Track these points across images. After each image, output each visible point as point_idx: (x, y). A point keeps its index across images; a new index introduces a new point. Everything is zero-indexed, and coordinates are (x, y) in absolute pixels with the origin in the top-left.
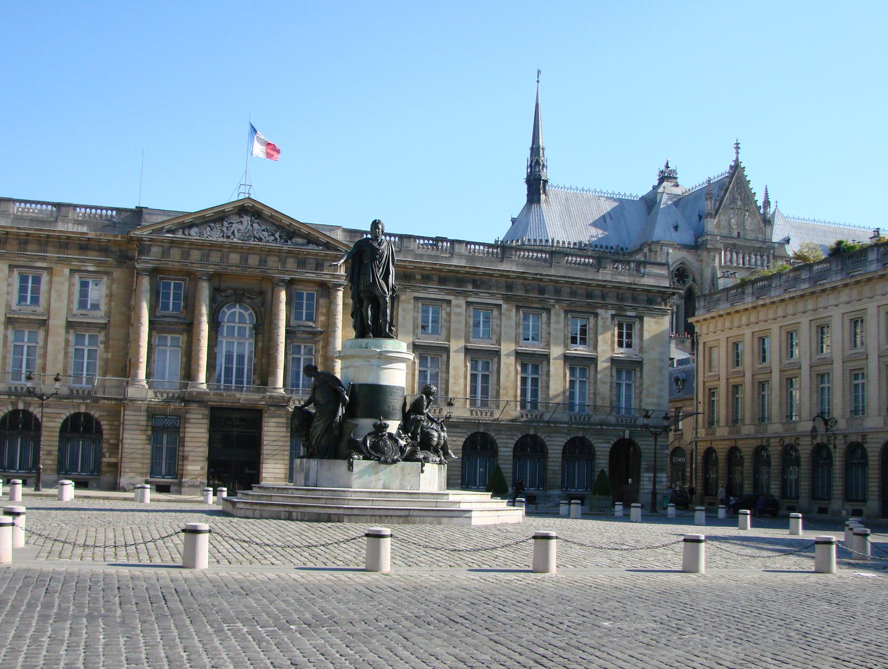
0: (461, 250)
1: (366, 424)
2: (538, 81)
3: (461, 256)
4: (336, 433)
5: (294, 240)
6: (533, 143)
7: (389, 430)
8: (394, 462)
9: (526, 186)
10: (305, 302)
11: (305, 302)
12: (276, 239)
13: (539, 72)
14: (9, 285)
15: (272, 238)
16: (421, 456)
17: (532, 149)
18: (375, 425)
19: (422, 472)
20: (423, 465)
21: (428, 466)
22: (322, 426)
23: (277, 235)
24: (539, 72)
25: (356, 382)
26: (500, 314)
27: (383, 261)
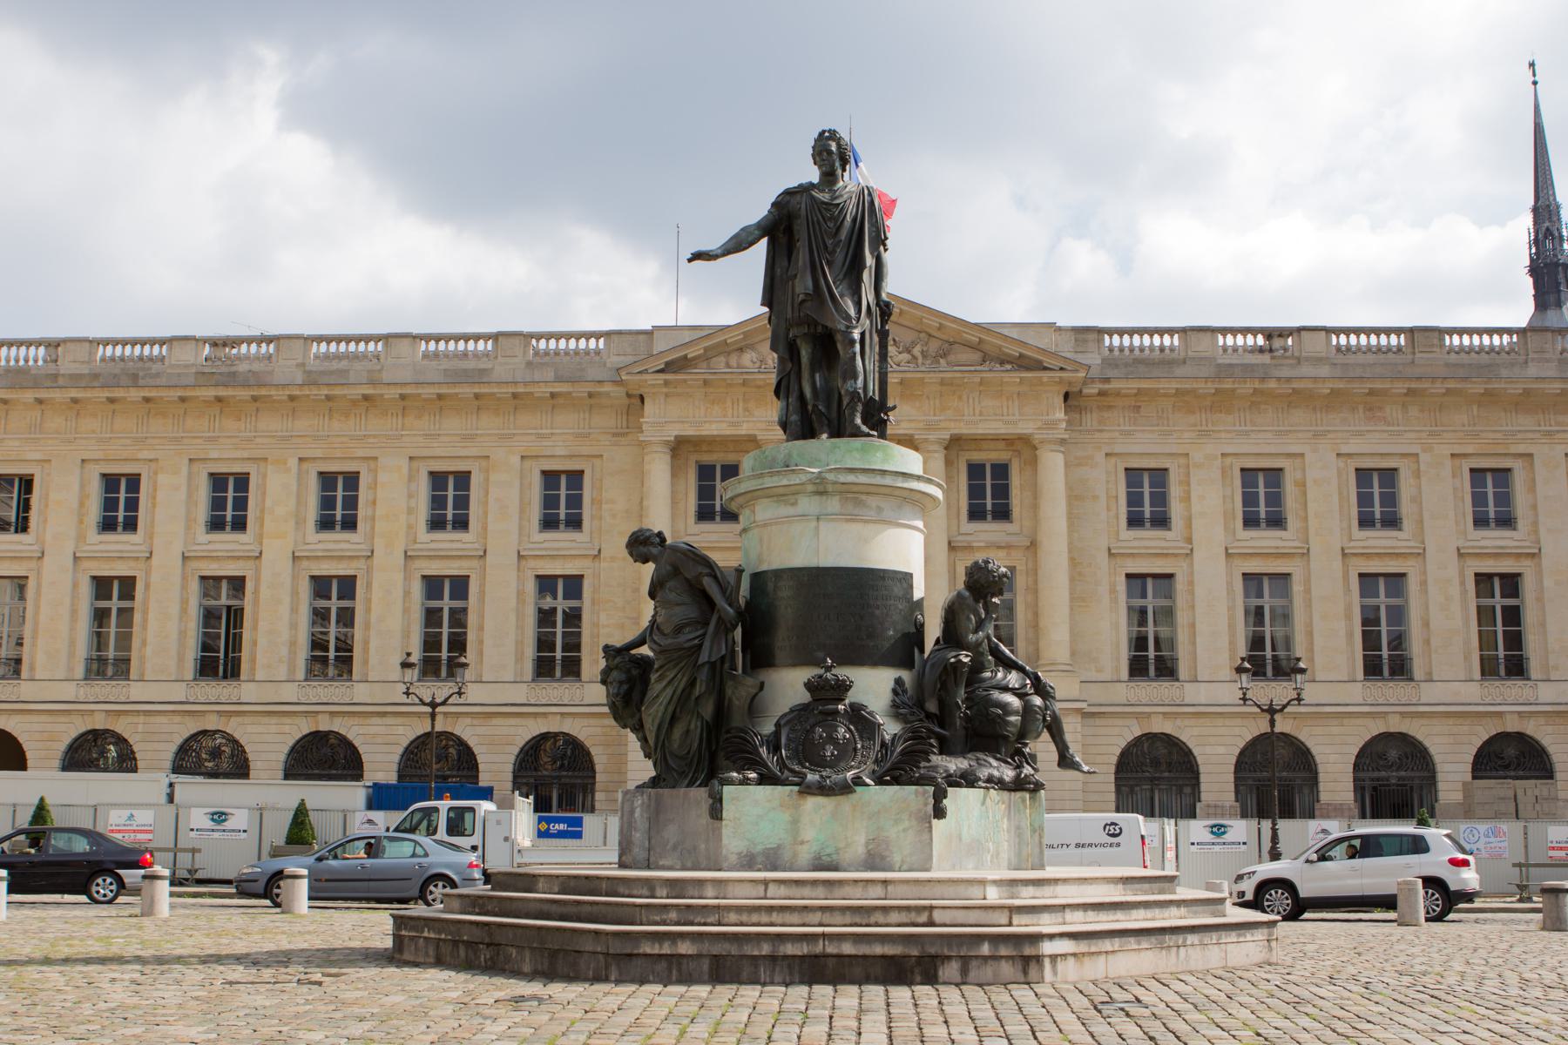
0: (1314, 345)
1: (789, 686)
2: (1535, 83)
3: (1319, 361)
4: (708, 710)
5: (952, 358)
6: (1537, 198)
7: (852, 697)
8: (845, 789)
9: (1530, 281)
10: (988, 482)
11: (988, 482)
12: (914, 357)
13: (1532, 65)
14: (410, 496)
15: (906, 356)
16: (955, 764)
17: (1535, 210)
18: (809, 686)
19: (939, 813)
20: (940, 795)
21: (957, 799)
22: (669, 691)
23: (917, 351)
24: (1532, 65)
25: (764, 567)
26: (1417, 474)
27: (844, 234)
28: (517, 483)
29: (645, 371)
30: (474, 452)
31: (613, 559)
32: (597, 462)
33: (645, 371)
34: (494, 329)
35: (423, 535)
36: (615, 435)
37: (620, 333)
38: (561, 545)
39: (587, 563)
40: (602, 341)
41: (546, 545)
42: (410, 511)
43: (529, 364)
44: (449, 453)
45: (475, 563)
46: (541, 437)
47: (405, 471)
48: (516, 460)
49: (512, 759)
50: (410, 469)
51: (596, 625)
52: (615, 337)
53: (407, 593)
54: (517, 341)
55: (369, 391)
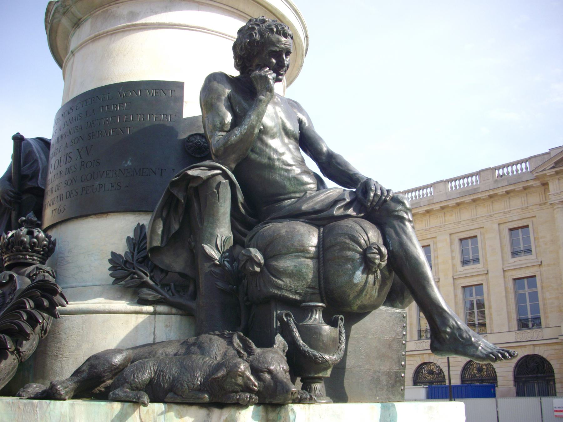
28: (498, 237)
29: (545, 170)
30: (477, 226)
31: (549, 265)
32: (534, 219)
33: (545, 170)
34: (477, 170)
35: (460, 268)
36: (541, 205)
37: (535, 157)
38: (523, 262)
39: (536, 269)
40: (527, 163)
41: (516, 263)
42: (453, 258)
43: (496, 181)
44: (465, 229)
45: (484, 277)
46: (505, 213)
47: (448, 240)
48: (496, 226)
49: (512, 369)
50: (451, 239)
51: (544, 299)
52: (533, 160)
53: (456, 296)
54: (489, 172)
55: (428, 208)
